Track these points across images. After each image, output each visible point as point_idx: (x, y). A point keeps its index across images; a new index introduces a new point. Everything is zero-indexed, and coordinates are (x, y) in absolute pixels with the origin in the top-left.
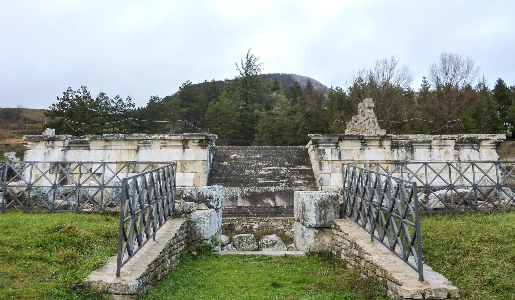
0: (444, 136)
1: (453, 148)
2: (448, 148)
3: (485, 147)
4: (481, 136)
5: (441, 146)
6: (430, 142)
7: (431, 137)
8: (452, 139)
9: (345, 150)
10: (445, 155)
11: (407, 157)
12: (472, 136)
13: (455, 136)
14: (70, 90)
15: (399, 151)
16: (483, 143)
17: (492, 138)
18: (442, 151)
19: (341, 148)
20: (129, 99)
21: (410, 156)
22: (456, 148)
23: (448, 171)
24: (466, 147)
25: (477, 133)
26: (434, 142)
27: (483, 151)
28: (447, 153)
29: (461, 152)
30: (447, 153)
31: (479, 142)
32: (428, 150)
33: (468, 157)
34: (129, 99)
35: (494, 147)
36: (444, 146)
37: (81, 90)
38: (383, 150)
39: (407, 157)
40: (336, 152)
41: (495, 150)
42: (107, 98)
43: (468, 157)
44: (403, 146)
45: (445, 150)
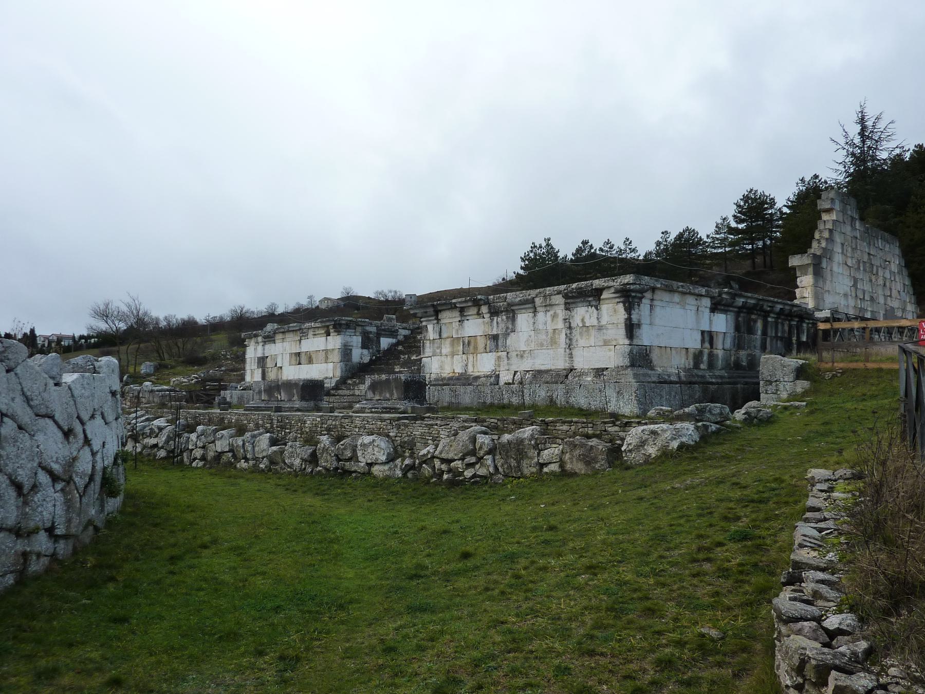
0: (548, 290)
1: (563, 307)
2: (556, 308)
3: (607, 301)
4: (597, 283)
5: (548, 306)
6: (532, 301)
7: (533, 293)
8: (559, 293)
9: (445, 324)
10: (553, 320)
11: (507, 328)
12: (583, 284)
13: (562, 287)
14: (535, 247)
15: (499, 319)
16: (605, 295)
17: (611, 284)
18: (549, 314)
19: (442, 321)
20: (628, 242)
21: (510, 326)
22: (568, 307)
23: (61, 423)
24: (580, 305)
25: (591, 279)
26: (538, 301)
27: (605, 308)
28: (554, 316)
29: (573, 314)
30: (554, 316)
31: (598, 293)
32: (531, 315)
33: (583, 320)
34: (628, 242)
35: (622, 300)
36: (551, 305)
37: (544, 244)
38: (481, 320)
39: (507, 328)
40: (437, 329)
41: (621, 305)
42: (591, 247)
43: (583, 320)
44: (502, 312)
45: (552, 312)
